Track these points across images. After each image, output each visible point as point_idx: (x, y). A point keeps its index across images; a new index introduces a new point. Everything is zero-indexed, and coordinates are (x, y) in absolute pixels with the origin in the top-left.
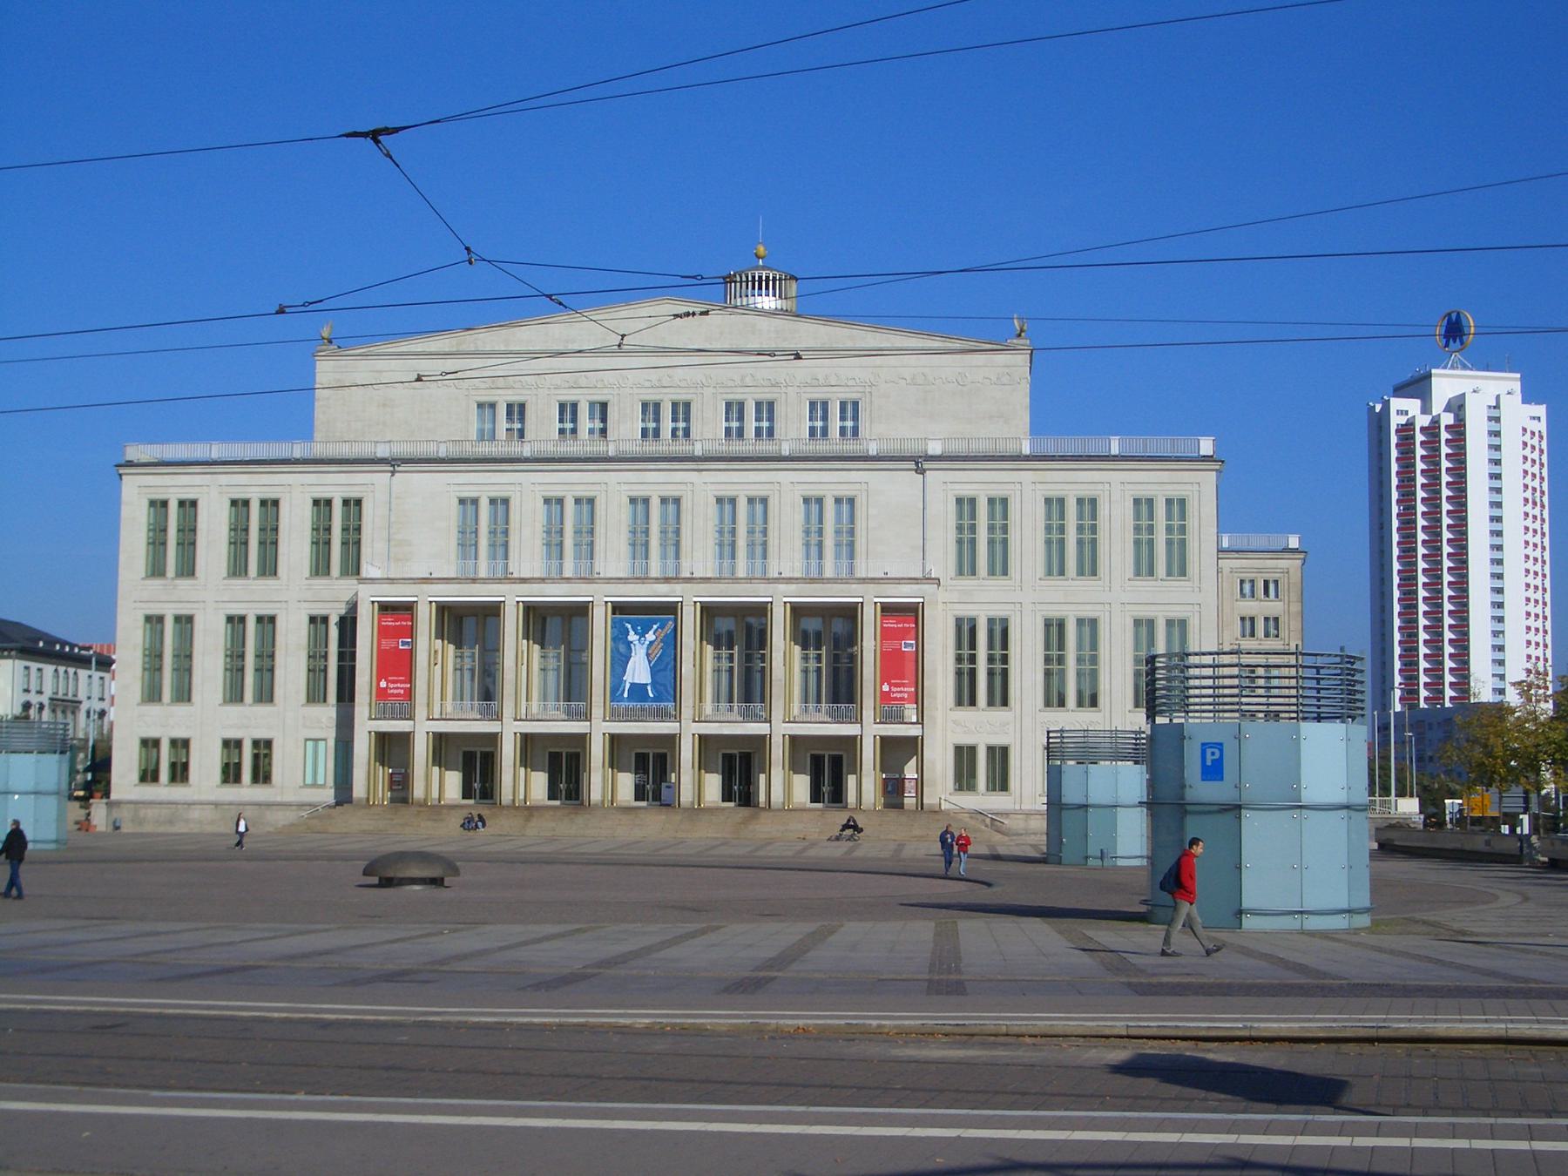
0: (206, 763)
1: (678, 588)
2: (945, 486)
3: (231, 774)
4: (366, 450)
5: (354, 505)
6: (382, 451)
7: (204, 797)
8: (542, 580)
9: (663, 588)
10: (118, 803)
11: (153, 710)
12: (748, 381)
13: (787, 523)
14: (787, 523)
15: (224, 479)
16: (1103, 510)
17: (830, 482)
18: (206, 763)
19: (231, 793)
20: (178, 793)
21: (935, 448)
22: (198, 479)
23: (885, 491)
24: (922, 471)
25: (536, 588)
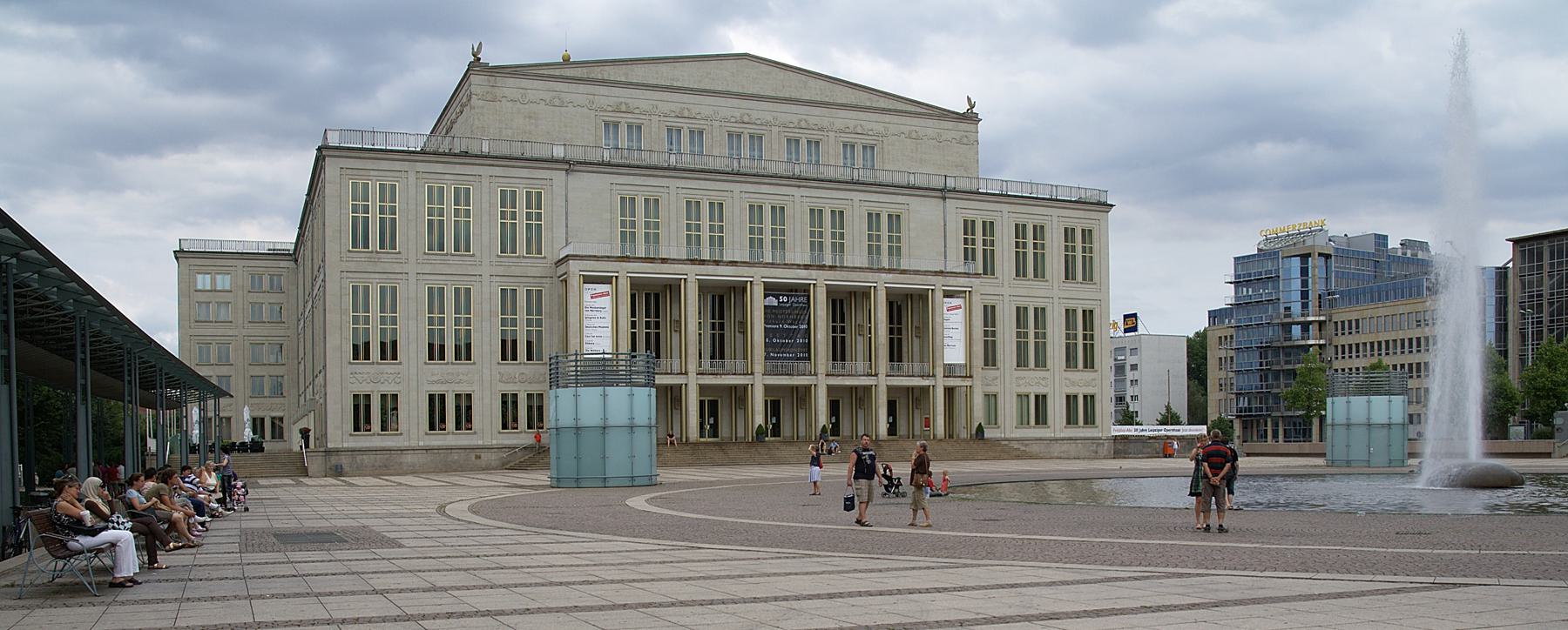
0: (413, 413)
1: (814, 273)
2: (957, 212)
3: (436, 420)
4: (543, 152)
5: (535, 200)
6: (559, 152)
7: (413, 443)
8: (806, 267)
9: (803, 273)
10: (337, 451)
11: (363, 368)
12: (803, 124)
13: (856, 230)
14: (856, 230)
15: (420, 167)
16: (1047, 235)
17: (885, 204)
18: (413, 413)
19: (437, 440)
20: (389, 441)
21: (951, 183)
22: (397, 166)
23: (921, 214)
24: (944, 198)
25: (710, 269)
